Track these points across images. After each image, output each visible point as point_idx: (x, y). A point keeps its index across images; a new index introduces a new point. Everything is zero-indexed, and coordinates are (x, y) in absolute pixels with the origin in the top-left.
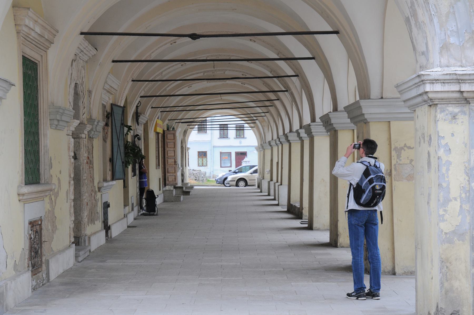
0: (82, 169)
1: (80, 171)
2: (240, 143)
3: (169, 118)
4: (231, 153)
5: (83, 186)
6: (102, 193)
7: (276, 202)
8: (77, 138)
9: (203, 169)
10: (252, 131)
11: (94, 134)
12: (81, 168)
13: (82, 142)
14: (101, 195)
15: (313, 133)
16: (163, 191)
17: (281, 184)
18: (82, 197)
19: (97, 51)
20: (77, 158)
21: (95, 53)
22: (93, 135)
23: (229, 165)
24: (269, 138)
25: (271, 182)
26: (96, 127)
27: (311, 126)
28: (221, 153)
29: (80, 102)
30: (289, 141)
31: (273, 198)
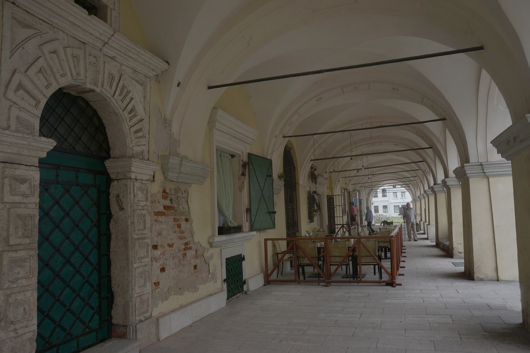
0: (130, 225)
2: (404, 201)
3: (352, 182)
6: (221, 248)
7: (425, 236)
8: (123, 179)
9: (385, 214)
10: (408, 192)
11: (179, 176)
15: (467, 175)
17: (429, 224)
18: (130, 265)
19: (169, 64)
20: (124, 207)
21: (167, 68)
24: (418, 194)
25: (421, 222)
27: (465, 167)
28: (394, 206)
29: (124, 126)
30: (434, 191)
31: (423, 232)
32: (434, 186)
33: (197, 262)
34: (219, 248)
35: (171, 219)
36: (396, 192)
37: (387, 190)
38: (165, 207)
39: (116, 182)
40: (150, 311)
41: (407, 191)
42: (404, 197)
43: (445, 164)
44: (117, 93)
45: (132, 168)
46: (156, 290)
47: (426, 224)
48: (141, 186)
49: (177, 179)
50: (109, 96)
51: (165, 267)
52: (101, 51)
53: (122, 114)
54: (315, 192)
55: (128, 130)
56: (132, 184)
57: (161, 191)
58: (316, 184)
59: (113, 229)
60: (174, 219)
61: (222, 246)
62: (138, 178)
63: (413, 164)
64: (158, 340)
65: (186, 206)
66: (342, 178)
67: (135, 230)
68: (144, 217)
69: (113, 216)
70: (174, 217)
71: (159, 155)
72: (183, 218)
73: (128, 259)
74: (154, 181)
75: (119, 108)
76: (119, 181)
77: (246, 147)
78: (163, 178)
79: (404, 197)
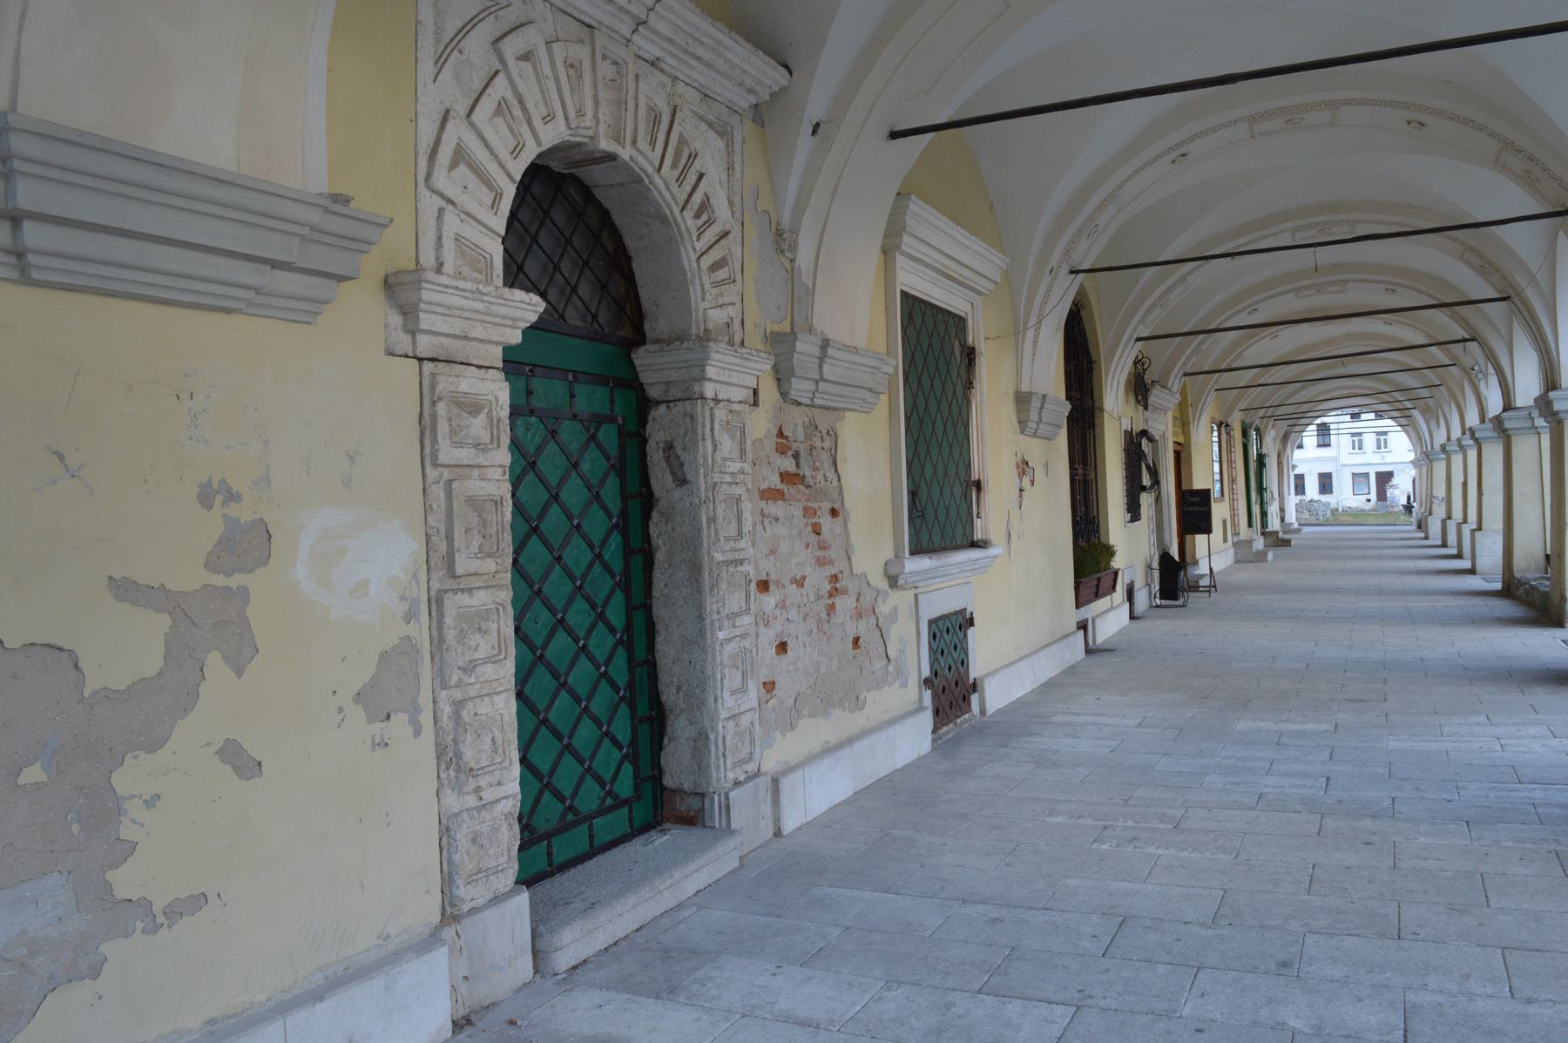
0: (704, 523)
1: (699, 530)
2: (1383, 458)
4: (1368, 474)
5: (712, 590)
7: (1465, 564)
8: (684, 400)
9: (1325, 498)
10: (1403, 433)
11: (817, 390)
12: (704, 518)
13: (703, 413)
14: (916, 596)
16: (1233, 543)
17: (1480, 528)
18: (708, 635)
19: (791, 73)
20: (688, 477)
21: (784, 82)
22: (814, 394)
23: (1367, 491)
24: (1440, 437)
25: (1448, 522)
26: (820, 366)
28: (1354, 474)
29: (683, 253)
31: (1454, 551)
32: (1505, 414)
33: (863, 628)
34: (912, 592)
35: (796, 510)
36: (1360, 434)
37: (1332, 426)
38: (785, 477)
39: (662, 408)
40: (758, 757)
41: (1399, 429)
42: (1386, 447)
43: (1545, 342)
44: (668, 161)
45: (708, 368)
46: (767, 702)
47: (1466, 530)
48: (730, 417)
49: (812, 399)
50: (650, 170)
51: (785, 642)
52: (627, 46)
53: (679, 218)
54: (1144, 433)
55: (695, 264)
56: (707, 413)
57: (775, 432)
58: (1146, 408)
59: (658, 537)
60: (805, 509)
61: (918, 584)
62: (720, 397)
63: (1434, 349)
64: (778, 833)
65: (831, 474)
66: (1217, 390)
67: (719, 540)
68: (737, 504)
69: (658, 500)
70: (805, 504)
71: (766, 332)
72: (827, 506)
73: (701, 618)
74: (756, 403)
75: (672, 202)
76: (672, 405)
77: (972, 304)
78: (776, 395)
79: (1386, 447)
